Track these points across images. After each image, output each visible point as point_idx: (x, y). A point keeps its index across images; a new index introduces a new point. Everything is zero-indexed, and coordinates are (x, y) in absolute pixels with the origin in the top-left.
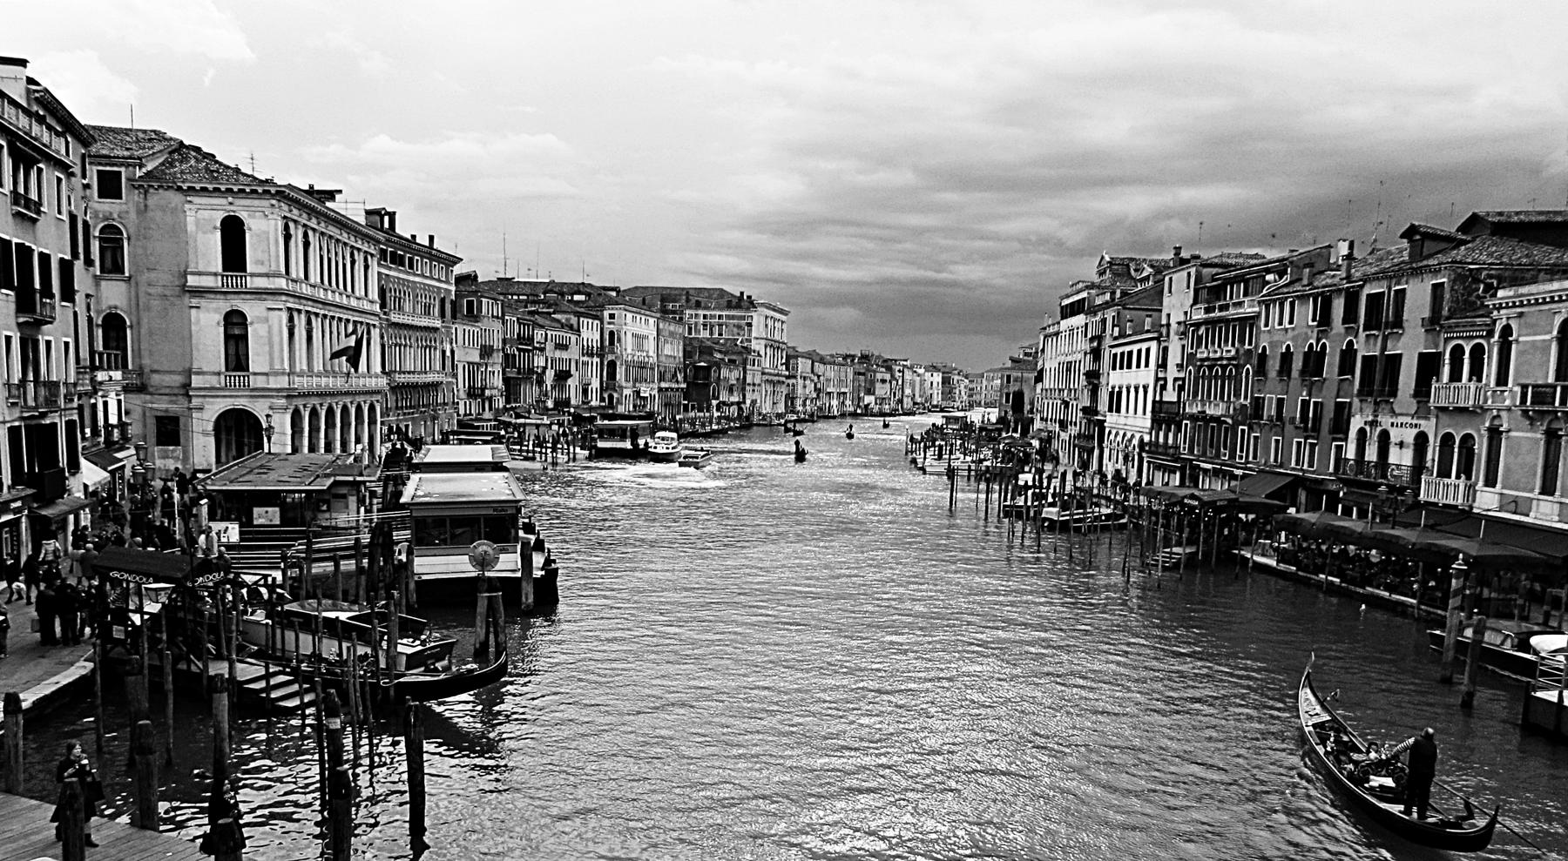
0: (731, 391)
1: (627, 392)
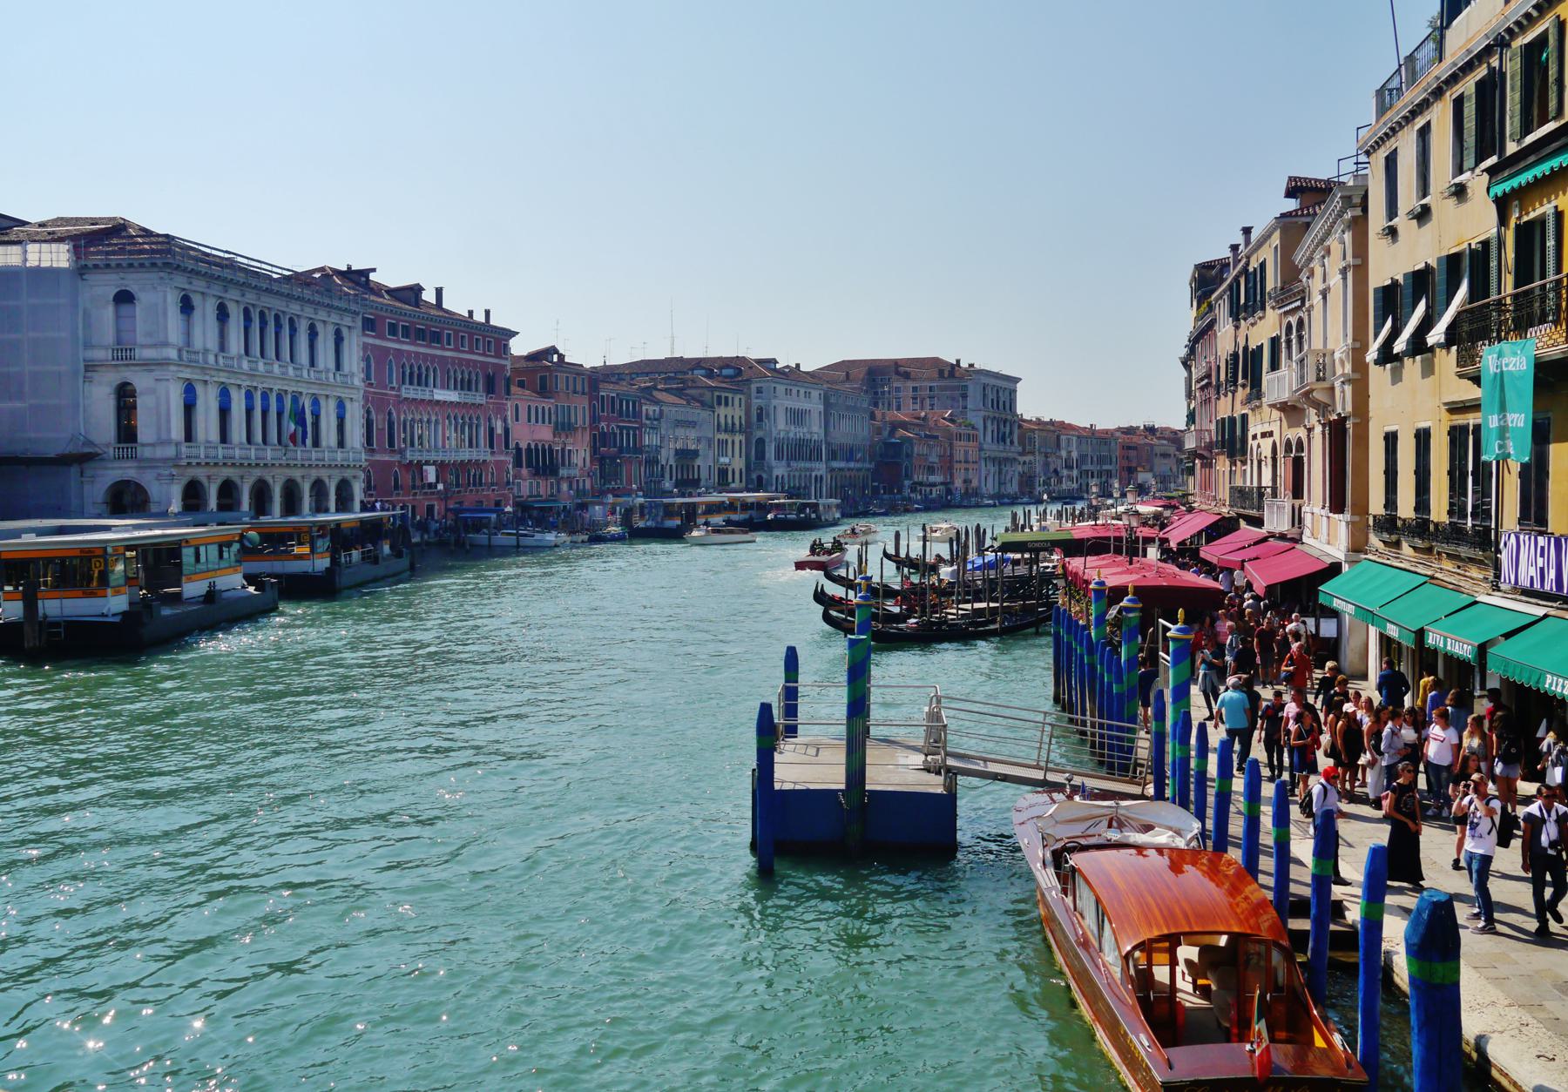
1: (780, 470)
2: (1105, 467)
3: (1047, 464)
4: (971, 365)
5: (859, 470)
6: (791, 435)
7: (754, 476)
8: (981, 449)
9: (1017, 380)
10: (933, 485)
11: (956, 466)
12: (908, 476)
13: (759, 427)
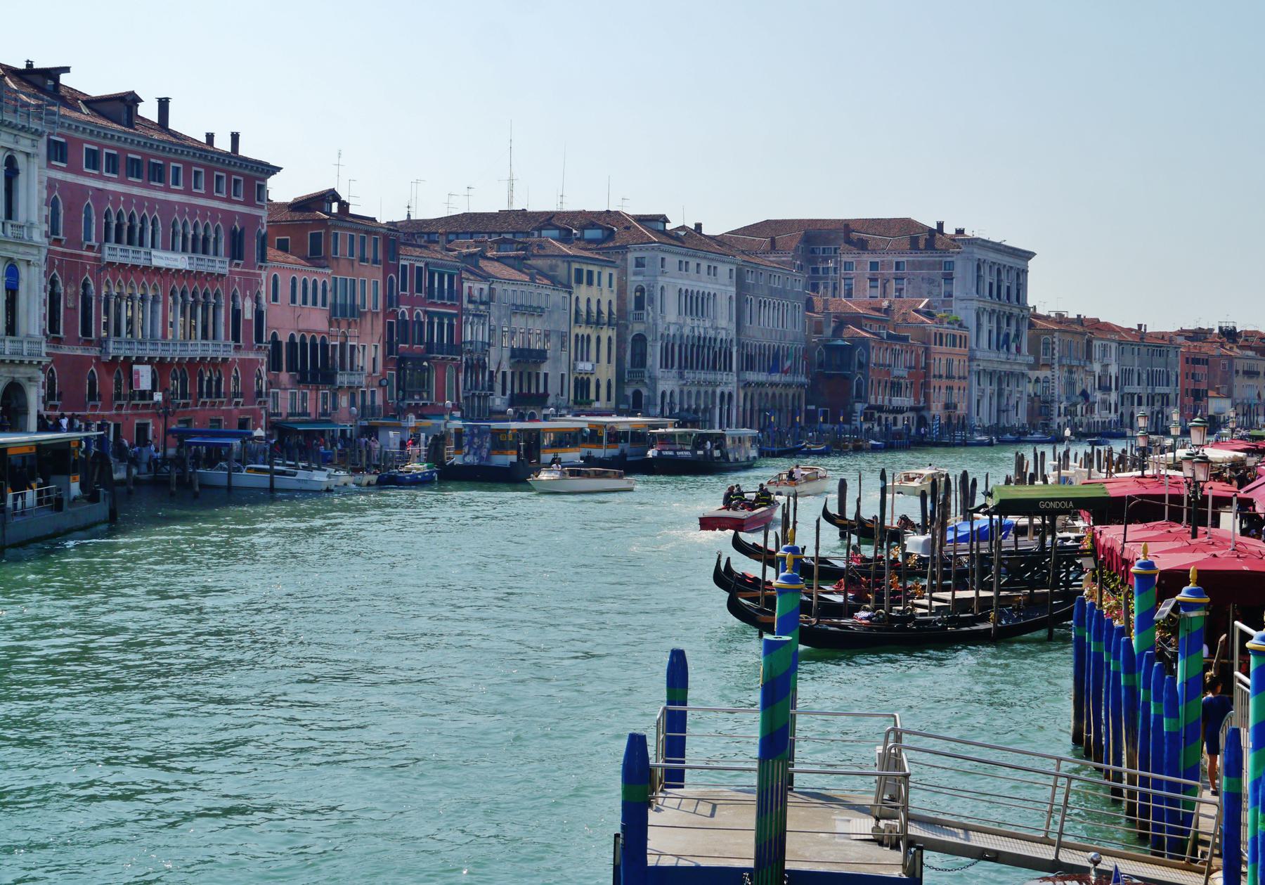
0: (896, 388)
1: (667, 383)
2: (1158, 390)
3: (1071, 384)
4: (960, 232)
5: (787, 385)
6: (687, 331)
7: (629, 391)
8: (971, 359)
9: (1029, 255)
10: (899, 410)
11: (935, 382)
12: (861, 397)
13: (639, 318)
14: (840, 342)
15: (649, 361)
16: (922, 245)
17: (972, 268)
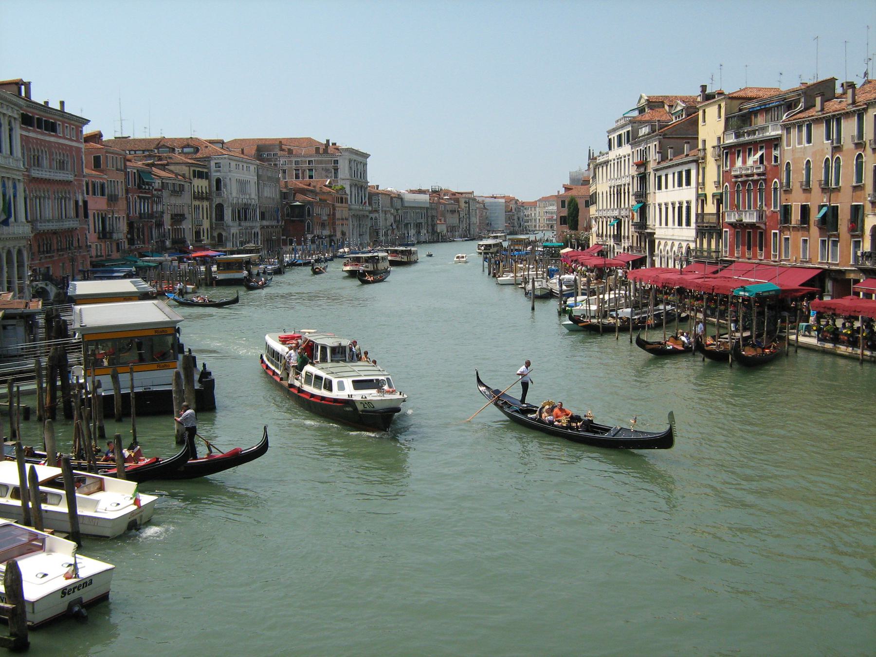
0: (323, 225)
3: (386, 220)
7: (215, 234)
14: (298, 203)
15: (226, 218)
16: (321, 151)
17: (347, 162)
